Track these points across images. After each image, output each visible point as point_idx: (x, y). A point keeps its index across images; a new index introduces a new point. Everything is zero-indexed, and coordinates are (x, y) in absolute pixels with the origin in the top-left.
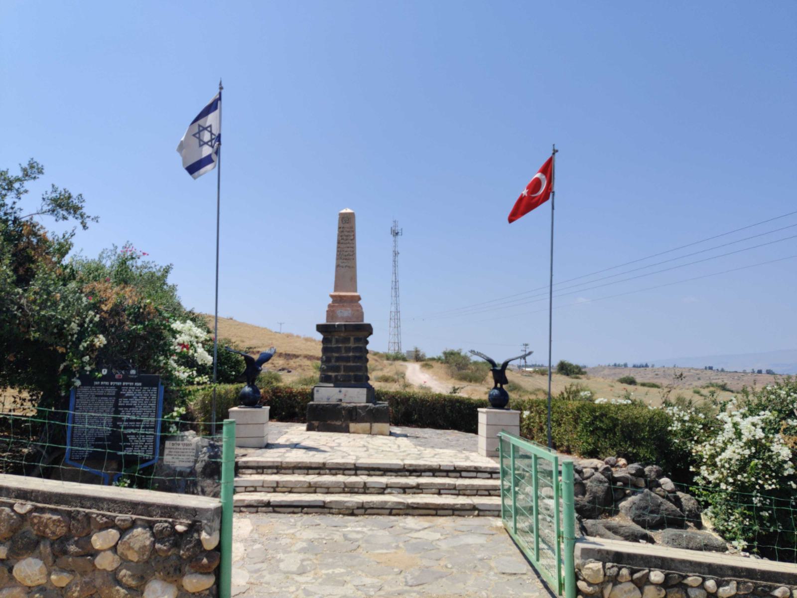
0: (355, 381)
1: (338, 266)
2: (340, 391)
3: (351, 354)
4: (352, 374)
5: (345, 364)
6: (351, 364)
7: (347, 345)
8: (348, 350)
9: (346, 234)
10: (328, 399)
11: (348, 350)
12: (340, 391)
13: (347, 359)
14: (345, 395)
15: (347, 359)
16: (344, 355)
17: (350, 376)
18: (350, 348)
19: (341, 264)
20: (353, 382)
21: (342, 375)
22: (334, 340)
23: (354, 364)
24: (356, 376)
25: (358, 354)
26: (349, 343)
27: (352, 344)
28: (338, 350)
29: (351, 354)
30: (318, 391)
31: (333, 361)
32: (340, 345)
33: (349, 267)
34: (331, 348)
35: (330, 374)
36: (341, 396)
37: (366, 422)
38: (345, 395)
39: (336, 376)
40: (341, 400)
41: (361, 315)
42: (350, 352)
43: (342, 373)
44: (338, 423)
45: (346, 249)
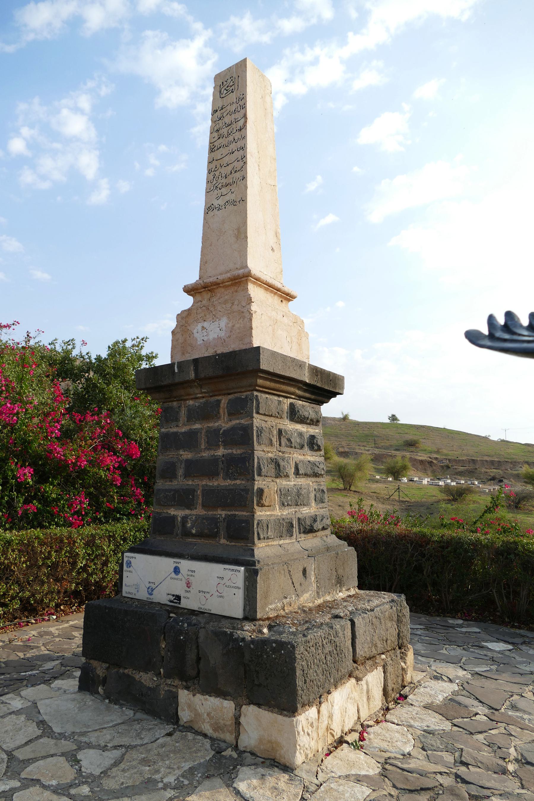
0: (231, 537)
1: (209, 209)
2: (177, 570)
3: (221, 452)
4: (222, 513)
5: (205, 482)
6: (221, 482)
7: (211, 425)
8: (214, 438)
9: (227, 120)
10: (151, 591)
11: (214, 438)
12: (177, 570)
13: (208, 469)
14: (188, 585)
15: (208, 469)
16: (205, 454)
17: (214, 520)
18: (217, 430)
19: (216, 203)
20: (223, 541)
21: (198, 517)
22: (183, 413)
23: (228, 482)
24: (231, 521)
25: (237, 451)
26: (217, 417)
27: (224, 423)
28: (190, 440)
29: (221, 452)
30: (129, 564)
31: (180, 472)
32: (197, 426)
33: (234, 203)
34: (176, 434)
35: (172, 512)
36: (179, 588)
37: (222, 694)
38: (188, 585)
39: (185, 519)
40: (178, 598)
41: (248, 332)
42: (218, 446)
43: (199, 511)
44: (147, 679)
45: (226, 160)
